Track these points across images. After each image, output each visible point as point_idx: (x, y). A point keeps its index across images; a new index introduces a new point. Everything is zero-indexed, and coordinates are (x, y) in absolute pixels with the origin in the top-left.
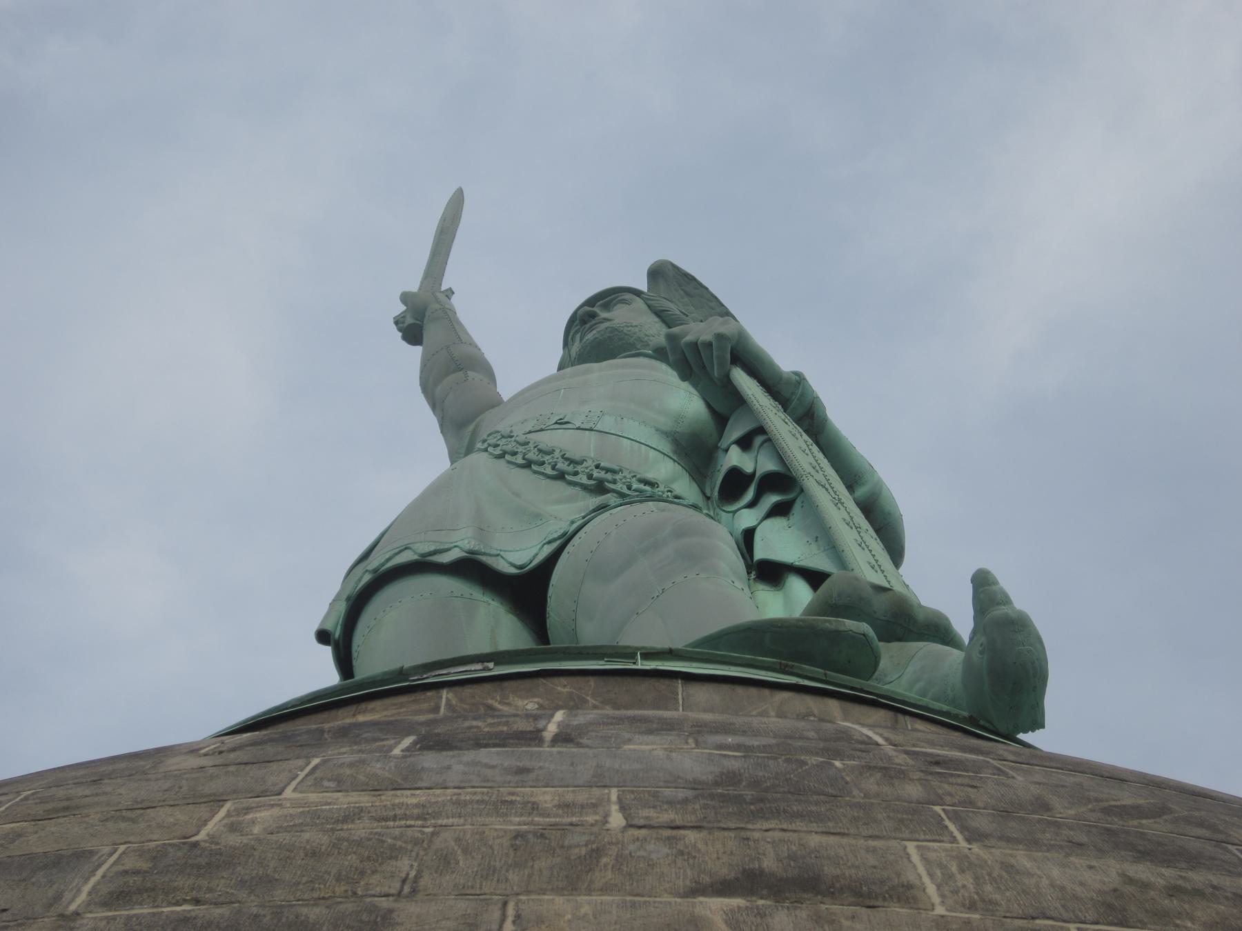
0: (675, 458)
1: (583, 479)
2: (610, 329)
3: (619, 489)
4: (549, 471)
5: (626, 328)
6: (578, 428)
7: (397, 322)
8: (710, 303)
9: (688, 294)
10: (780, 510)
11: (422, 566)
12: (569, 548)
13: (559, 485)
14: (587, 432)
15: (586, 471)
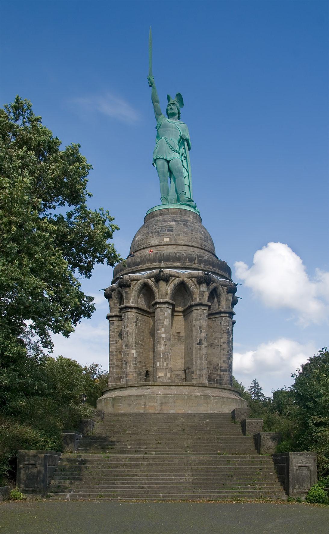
10: (185, 159)
11: (163, 158)
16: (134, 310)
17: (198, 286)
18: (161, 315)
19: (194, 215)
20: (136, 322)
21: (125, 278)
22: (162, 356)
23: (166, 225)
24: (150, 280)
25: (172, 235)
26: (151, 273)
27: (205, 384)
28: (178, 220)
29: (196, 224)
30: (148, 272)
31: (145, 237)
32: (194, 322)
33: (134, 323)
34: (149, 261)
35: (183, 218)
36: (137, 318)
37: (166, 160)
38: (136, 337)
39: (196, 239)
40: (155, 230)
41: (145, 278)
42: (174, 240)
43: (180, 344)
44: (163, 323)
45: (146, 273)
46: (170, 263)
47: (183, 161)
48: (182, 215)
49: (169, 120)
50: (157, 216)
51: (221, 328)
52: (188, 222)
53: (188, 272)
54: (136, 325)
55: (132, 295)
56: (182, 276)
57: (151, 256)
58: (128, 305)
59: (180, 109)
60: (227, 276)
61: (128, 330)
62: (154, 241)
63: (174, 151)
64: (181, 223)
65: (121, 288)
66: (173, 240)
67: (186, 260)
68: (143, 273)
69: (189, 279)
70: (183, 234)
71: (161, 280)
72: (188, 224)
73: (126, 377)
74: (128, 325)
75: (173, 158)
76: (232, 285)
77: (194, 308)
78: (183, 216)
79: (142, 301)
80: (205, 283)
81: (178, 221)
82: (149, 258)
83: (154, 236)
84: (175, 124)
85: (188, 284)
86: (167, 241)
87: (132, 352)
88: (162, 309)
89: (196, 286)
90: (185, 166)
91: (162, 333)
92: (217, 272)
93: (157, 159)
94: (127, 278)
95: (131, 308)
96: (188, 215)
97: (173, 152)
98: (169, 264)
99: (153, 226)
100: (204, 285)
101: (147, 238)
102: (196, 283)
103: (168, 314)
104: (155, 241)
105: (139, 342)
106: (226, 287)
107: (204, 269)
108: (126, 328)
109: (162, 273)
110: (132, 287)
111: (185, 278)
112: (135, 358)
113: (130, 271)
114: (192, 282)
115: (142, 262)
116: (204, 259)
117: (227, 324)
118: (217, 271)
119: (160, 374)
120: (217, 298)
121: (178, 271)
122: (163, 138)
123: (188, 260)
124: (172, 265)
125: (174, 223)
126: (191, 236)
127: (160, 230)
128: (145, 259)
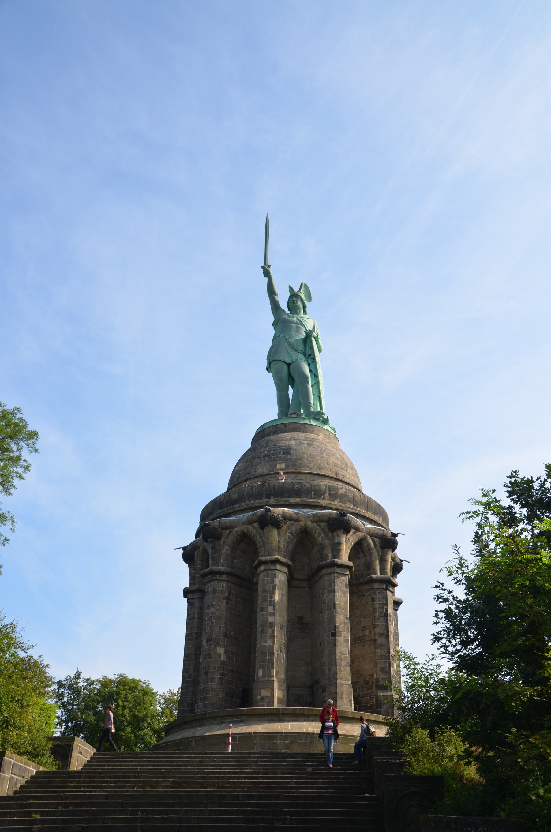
7: (262, 267)
10: (313, 362)
11: (280, 360)
16: (224, 577)
17: (330, 535)
18: (268, 583)
19: (326, 434)
20: (227, 598)
21: (212, 524)
22: (267, 658)
23: (280, 445)
24: (252, 526)
25: (289, 459)
26: (254, 514)
27: (346, 711)
28: (301, 438)
29: (328, 445)
30: (249, 514)
31: (249, 464)
32: (325, 595)
33: (224, 599)
34: (251, 496)
35: (308, 436)
36: (230, 593)
37: (285, 362)
38: (226, 624)
39: (327, 466)
40: (264, 453)
41: (243, 523)
42: (293, 466)
43: (304, 638)
44: (271, 597)
45: (246, 515)
46: (284, 499)
48: (306, 432)
50: (269, 434)
51: (374, 609)
52: (314, 441)
53: (313, 513)
54: (227, 603)
55: (224, 552)
56: (303, 519)
57: (254, 489)
58: (215, 568)
59: (307, 303)
60: (380, 521)
61: (213, 611)
62: (262, 469)
63: (296, 351)
64: (304, 442)
65: (207, 542)
66: (291, 466)
67: (310, 493)
68: (241, 516)
69: (315, 524)
70: (307, 457)
71: (269, 525)
72: (316, 444)
73: (205, 699)
74: (214, 603)
75: (295, 360)
76: (389, 535)
77: (325, 571)
78: (308, 434)
79: (240, 563)
80: (342, 531)
81: (299, 439)
82: (251, 492)
83: (263, 462)
84: (299, 318)
85: (313, 531)
86: (282, 467)
87: (218, 652)
88: (270, 572)
89: (327, 536)
90: (313, 370)
91: (268, 615)
92: (362, 514)
93: (272, 362)
94: (215, 524)
95: (221, 573)
96: (316, 432)
97: (296, 352)
98: (282, 500)
99: (261, 448)
100: (340, 532)
101: (252, 466)
102: (327, 530)
103: (280, 581)
104: (263, 469)
105: (232, 633)
106: (379, 538)
107: (340, 508)
108: (210, 608)
109: (269, 513)
110: (223, 539)
111: (308, 522)
112: (223, 663)
113: (221, 514)
114: (320, 529)
115: (241, 498)
116: (339, 493)
117: (385, 602)
118: (363, 511)
119: (264, 693)
120: (365, 556)
121: (296, 511)
123: (314, 494)
124: (287, 501)
125: (293, 443)
126: (319, 460)
127: (271, 452)
128: (245, 494)
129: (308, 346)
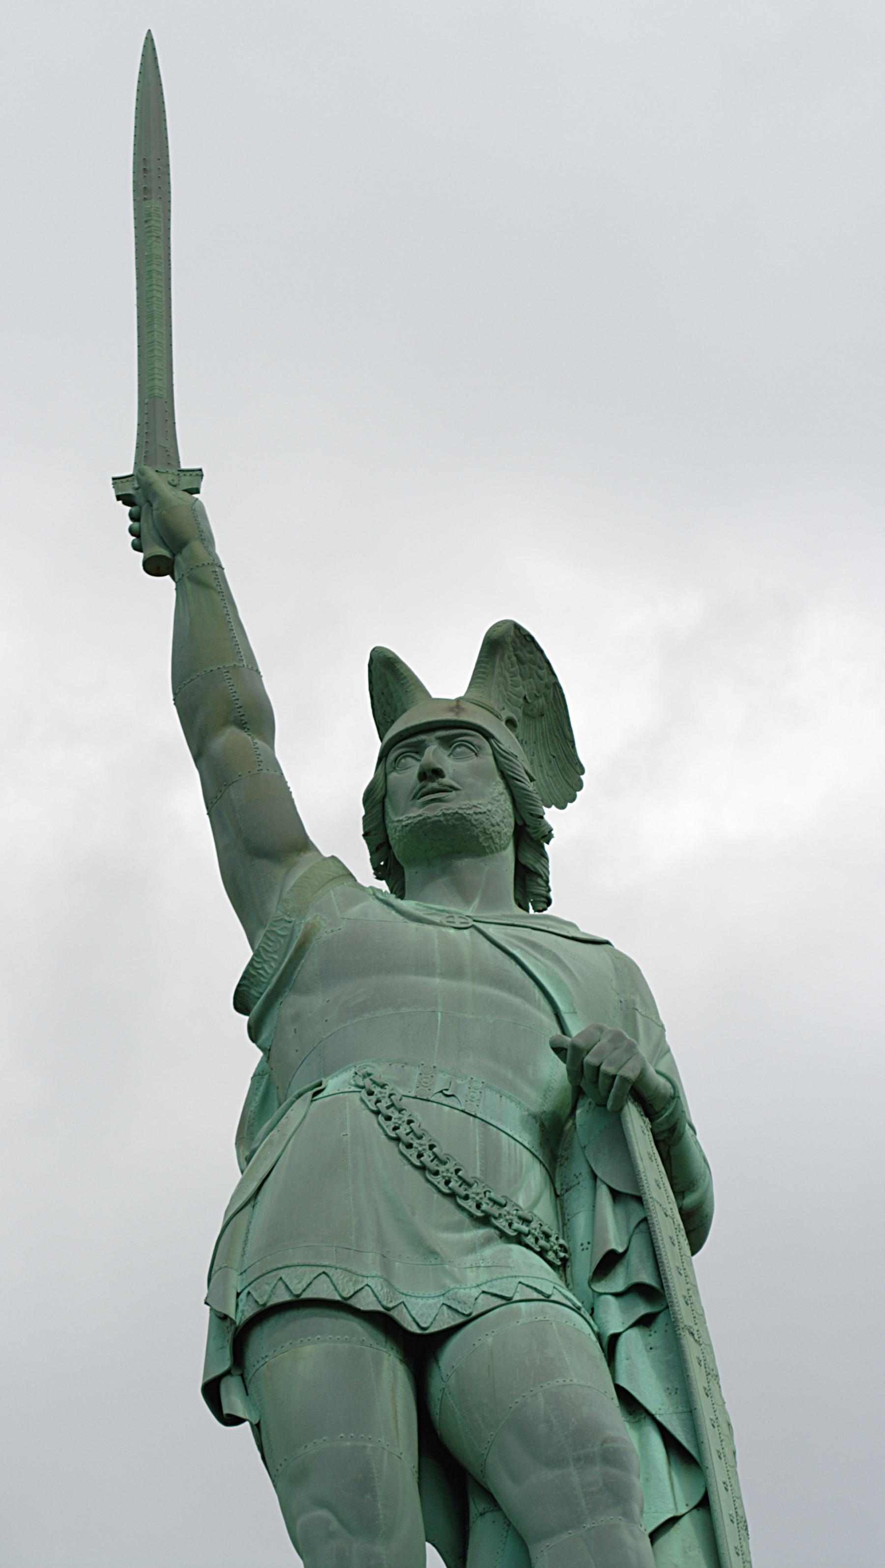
0: (541, 1158)
1: (470, 1205)
2: (457, 816)
3: (501, 1227)
4: (439, 1181)
5: (474, 815)
6: (463, 1111)
8: (540, 672)
9: (520, 661)
10: (645, 1322)
11: (342, 1306)
12: (469, 1327)
13: (447, 1204)
14: (472, 1118)
15: (477, 1198)
47: (615, 1337)
49: (406, 904)
63: (485, 1220)
84: (491, 930)
97: (482, 1232)
122: (332, 1085)
129: (585, 1181)
